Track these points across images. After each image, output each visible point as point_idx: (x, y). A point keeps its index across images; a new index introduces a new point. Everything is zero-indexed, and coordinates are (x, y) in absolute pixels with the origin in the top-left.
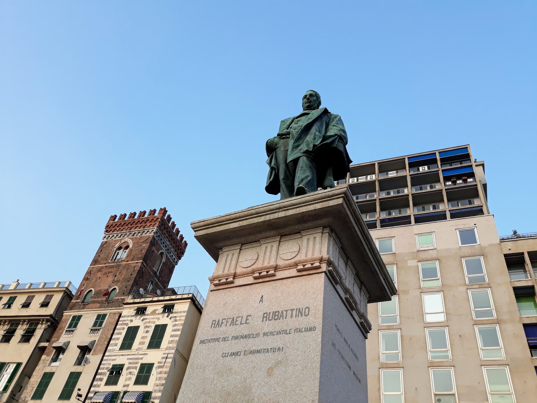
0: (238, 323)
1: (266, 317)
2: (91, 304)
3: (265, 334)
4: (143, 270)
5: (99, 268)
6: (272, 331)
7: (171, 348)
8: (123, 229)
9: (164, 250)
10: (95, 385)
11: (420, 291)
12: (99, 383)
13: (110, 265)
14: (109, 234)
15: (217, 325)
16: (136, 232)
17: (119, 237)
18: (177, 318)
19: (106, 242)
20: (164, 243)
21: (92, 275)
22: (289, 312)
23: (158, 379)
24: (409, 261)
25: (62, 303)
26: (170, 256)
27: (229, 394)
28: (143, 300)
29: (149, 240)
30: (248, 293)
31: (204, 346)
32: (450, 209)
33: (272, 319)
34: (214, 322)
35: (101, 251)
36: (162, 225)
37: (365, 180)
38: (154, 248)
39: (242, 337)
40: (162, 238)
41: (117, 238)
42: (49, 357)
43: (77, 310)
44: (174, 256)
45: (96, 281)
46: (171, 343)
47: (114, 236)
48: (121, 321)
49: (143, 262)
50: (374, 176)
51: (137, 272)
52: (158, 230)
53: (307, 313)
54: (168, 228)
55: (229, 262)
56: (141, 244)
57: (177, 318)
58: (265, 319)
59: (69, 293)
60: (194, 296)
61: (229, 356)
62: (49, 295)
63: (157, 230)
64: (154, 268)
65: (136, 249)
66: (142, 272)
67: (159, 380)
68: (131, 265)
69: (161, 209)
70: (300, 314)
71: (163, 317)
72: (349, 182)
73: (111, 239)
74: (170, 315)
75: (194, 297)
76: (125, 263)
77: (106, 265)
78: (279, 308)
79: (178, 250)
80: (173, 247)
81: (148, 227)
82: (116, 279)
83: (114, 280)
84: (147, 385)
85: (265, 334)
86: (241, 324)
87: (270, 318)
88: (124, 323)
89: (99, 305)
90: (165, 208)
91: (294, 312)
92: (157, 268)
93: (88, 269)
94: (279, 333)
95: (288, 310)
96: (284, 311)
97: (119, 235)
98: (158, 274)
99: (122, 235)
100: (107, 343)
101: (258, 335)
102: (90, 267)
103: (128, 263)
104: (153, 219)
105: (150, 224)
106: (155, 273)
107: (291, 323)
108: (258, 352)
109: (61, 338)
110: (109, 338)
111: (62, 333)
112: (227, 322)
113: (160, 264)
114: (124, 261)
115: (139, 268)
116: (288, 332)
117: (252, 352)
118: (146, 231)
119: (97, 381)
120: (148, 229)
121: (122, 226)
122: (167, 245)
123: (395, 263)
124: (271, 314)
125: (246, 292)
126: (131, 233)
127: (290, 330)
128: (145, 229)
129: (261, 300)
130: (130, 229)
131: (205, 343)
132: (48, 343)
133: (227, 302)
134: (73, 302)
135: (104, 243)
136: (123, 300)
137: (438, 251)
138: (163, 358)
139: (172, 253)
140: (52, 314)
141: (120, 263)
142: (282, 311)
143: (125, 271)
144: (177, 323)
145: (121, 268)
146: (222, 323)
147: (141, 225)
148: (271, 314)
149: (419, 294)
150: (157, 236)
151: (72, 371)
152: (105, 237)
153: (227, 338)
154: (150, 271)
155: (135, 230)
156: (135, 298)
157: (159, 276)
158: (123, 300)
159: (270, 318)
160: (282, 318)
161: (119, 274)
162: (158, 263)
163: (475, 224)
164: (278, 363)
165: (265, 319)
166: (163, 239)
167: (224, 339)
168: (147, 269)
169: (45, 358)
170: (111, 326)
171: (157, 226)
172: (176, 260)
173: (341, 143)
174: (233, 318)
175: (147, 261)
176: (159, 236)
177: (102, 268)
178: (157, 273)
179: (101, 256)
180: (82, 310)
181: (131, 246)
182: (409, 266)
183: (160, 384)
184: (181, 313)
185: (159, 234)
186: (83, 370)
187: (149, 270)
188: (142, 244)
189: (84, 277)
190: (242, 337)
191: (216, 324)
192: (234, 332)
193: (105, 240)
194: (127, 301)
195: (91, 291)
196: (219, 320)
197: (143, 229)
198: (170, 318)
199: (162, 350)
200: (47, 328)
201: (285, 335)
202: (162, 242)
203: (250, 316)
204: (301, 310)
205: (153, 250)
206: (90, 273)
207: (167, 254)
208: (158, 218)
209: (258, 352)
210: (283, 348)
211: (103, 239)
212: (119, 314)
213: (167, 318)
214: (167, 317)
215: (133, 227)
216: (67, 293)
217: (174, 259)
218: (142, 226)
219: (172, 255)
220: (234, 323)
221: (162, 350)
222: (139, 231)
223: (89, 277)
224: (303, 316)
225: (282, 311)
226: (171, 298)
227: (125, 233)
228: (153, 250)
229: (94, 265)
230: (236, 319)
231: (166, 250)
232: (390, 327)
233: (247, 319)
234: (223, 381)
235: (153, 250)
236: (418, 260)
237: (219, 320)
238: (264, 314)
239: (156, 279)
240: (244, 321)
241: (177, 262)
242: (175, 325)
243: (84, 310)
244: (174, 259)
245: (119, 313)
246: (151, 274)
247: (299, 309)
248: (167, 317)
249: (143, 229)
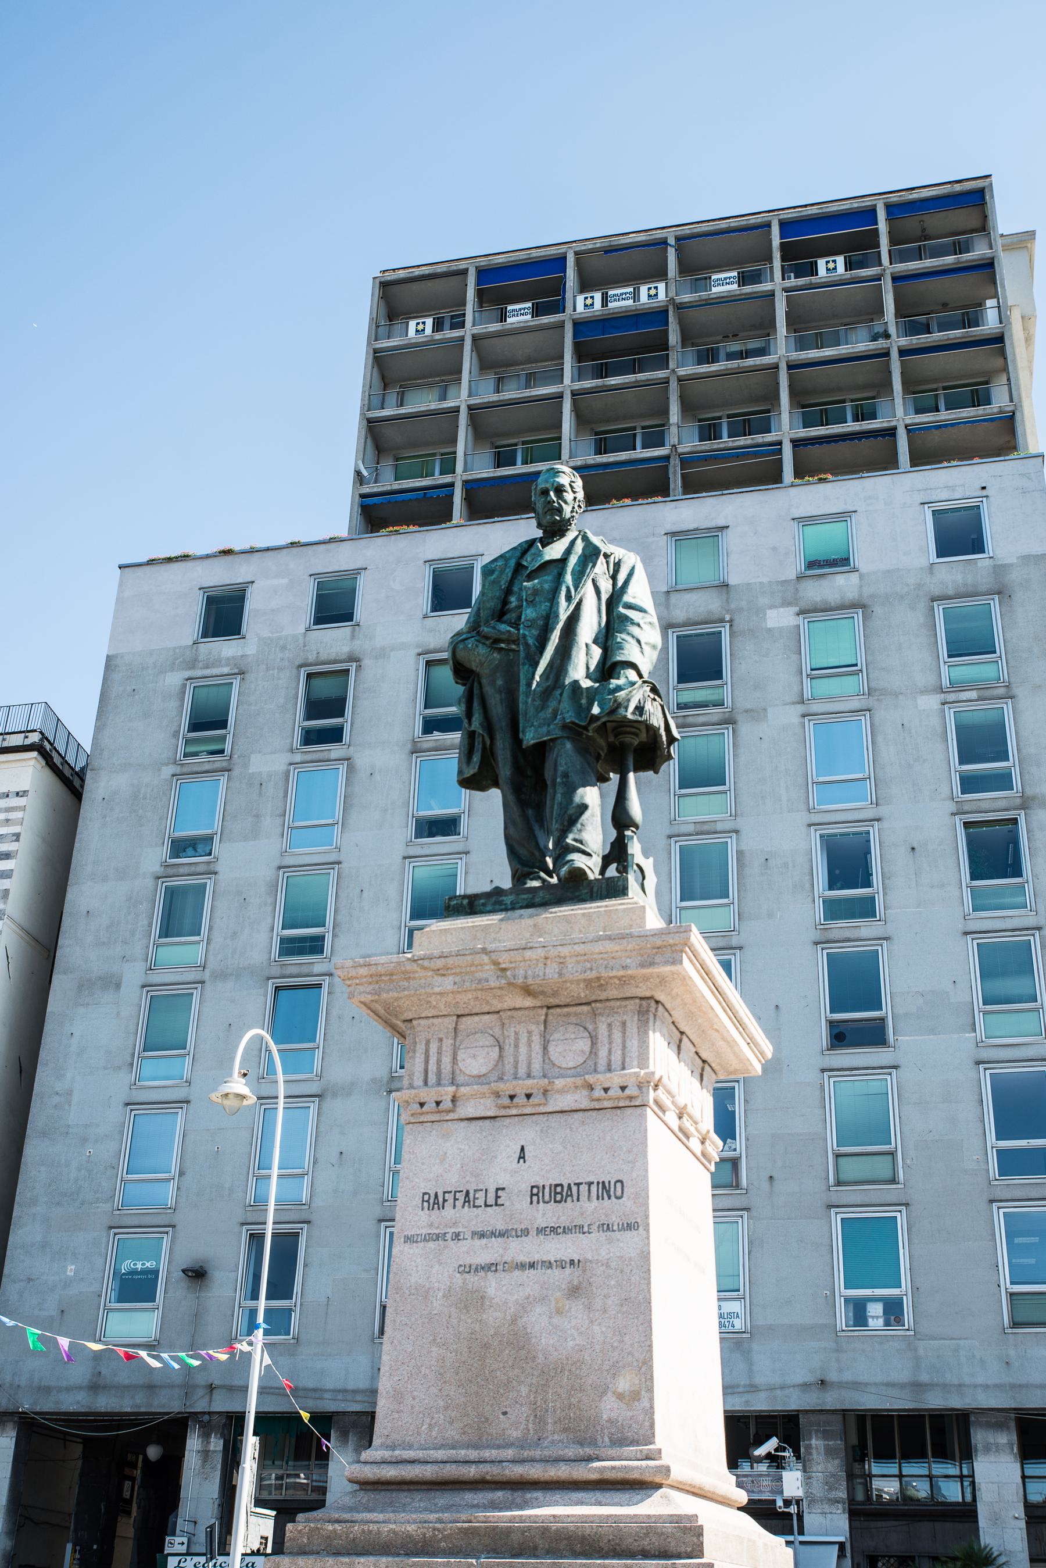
0: (480, 1202)
1: (536, 1193)
3: (540, 1231)
6: (553, 1225)
11: (801, 709)
15: (434, 1204)
22: (584, 1188)
24: (769, 612)
27: (486, 1346)
30: (490, 1138)
31: (416, 1249)
32: (908, 422)
33: (551, 1200)
34: (426, 1197)
37: (630, 302)
39: (493, 1234)
50: (662, 286)
53: (619, 1193)
55: (435, 1058)
58: (535, 1198)
61: (472, 1271)
70: (605, 1193)
72: (575, 310)
75: (46, 743)
78: (562, 1178)
85: (540, 1231)
86: (486, 1205)
87: (547, 1198)
91: (594, 1188)
94: (566, 1230)
95: (581, 1183)
96: (572, 1185)
101: (525, 1232)
107: (590, 1208)
108: (532, 1265)
112: (455, 1199)
116: (586, 1229)
117: (521, 1266)
123: (727, 618)
124: (547, 1190)
125: (484, 1134)
127: (589, 1225)
129: (522, 1157)
131: (417, 1242)
133: (446, 1153)
137: (861, 577)
142: (569, 1185)
146: (445, 1201)
148: (547, 1190)
149: (796, 720)
153: (462, 1234)
159: (547, 1198)
160: (569, 1199)
163: (984, 488)
164: (574, 1291)
165: (535, 1198)
167: (457, 1236)
173: (654, 700)
174: (468, 1192)
182: (770, 630)
184: (7, 800)
190: (493, 1234)
191: (432, 1201)
192: (474, 1222)
196: (436, 1193)
201: (581, 1235)
203: (503, 1189)
204: (607, 1185)
209: (532, 1265)
210: (579, 1261)
220: (472, 1203)
224: (613, 1198)
225: (569, 1185)
230: (474, 1195)
232: (706, 828)
233: (497, 1197)
234: (470, 1321)
236: (798, 608)
237: (436, 1193)
238: (532, 1187)
240: (491, 1200)
247: (603, 1182)
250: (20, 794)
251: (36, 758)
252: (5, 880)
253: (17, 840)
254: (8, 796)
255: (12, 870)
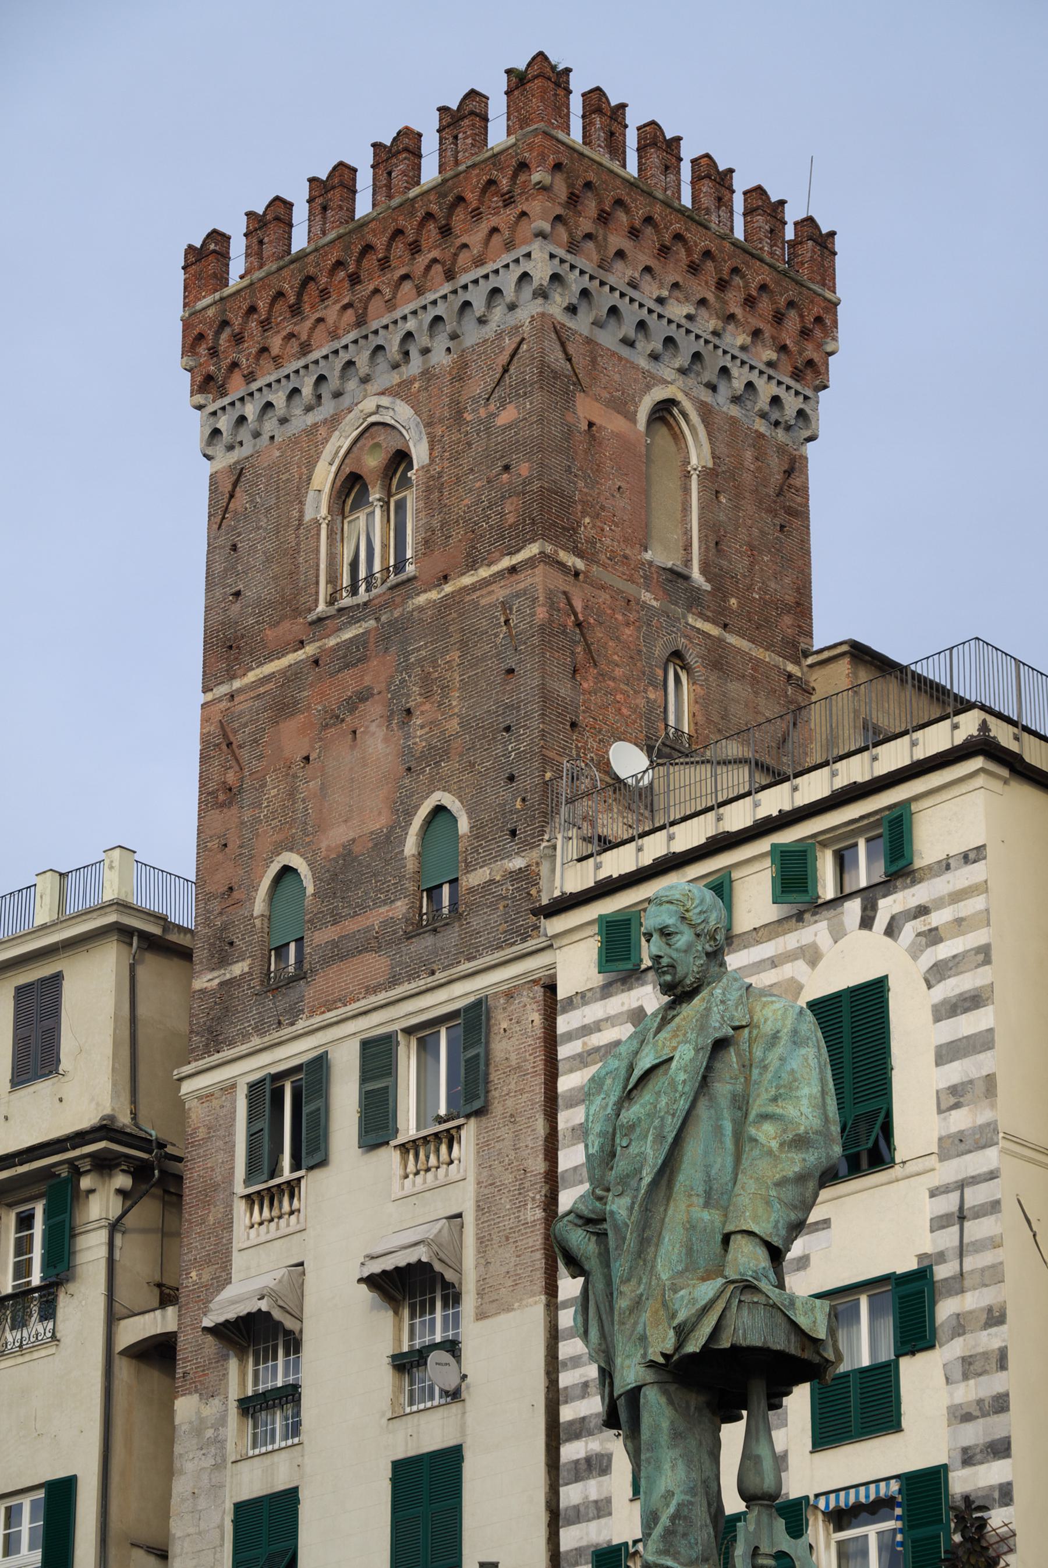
2: (332, 971)
4: (578, 605)
5: (271, 686)
7: (969, 1143)
8: (313, 328)
9: (666, 382)
10: (576, 1508)
12: (591, 1489)
13: (332, 642)
14: (232, 404)
16: (411, 325)
17: (309, 409)
18: (937, 919)
19: (238, 474)
20: (642, 325)
21: (244, 754)
23: (957, 1374)
25: (142, 1011)
26: (736, 400)
28: (655, 848)
29: (524, 370)
35: (234, 548)
36: (573, 200)
38: (586, 409)
40: (615, 299)
41: (301, 421)
42: (216, 1402)
43: (256, 1042)
44: (760, 383)
45: (292, 794)
46: (957, 1106)
47: (269, 405)
48: (570, 1036)
49: (549, 549)
51: (536, 640)
52: (561, 252)
54: (627, 200)
56: (483, 413)
57: (938, 918)
59: (155, 930)
60: (1000, 716)
62: (32, 984)
63: (552, 256)
64: (648, 556)
65: (466, 462)
66: (579, 625)
67: (966, 1377)
68: (475, 604)
69: (517, 80)
71: (838, 935)
73: (265, 437)
74: (882, 903)
76: (434, 595)
77: (310, 650)
79: (778, 318)
80: (731, 317)
81: (479, 262)
82: (419, 735)
83: (407, 752)
84: (902, 1430)
88: (597, 1049)
89: (376, 964)
90: (541, 54)
92: (676, 536)
93: (205, 720)
97: (307, 390)
98: (696, 574)
99: (322, 379)
100: (539, 1214)
102: (210, 696)
103: (448, 588)
104: (491, 182)
105: (484, 227)
106: (678, 577)
109: (238, 1261)
110: (540, 1179)
111: (228, 1225)
113: (686, 490)
114: (417, 584)
115: (541, 613)
118: (477, 297)
119: (577, 1479)
120: (486, 277)
121: (296, 310)
122: (672, 331)
126: (380, 348)
128: (465, 278)
130: (361, 321)
132: (171, 1310)
134: (203, 991)
135: (230, 488)
136: (527, 877)
138: (939, 1223)
139: (735, 372)
140: (108, 1111)
141: (396, 614)
143: (455, 655)
144: (944, 951)
145: (420, 648)
147: (422, 260)
150: (572, 309)
151: (400, 1455)
152: (216, 432)
154: (630, 589)
155: (397, 314)
156: (607, 845)
157: (708, 587)
158: (527, 877)
161: (427, 695)
162: (665, 487)
166: (623, 305)
168: (603, 587)
169: (198, 1412)
170: (522, 1092)
171: (541, 235)
172: (792, 404)
175: (572, 530)
176: (585, 293)
177: (291, 677)
178: (687, 578)
179: (249, 594)
180: (287, 1032)
181: (420, 453)
183: (980, 1402)
184: (948, 876)
185: (575, 282)
186: (463, 1429)
187: (620, 584)
188: (492, 407)
189: (202, 785)
193: (225, 460)
194: (552, 888)
195: (287, 871)
197: (446, 288)
198: (891, 931)
199: (911, 1168)
200: (119, 1212)
202: (628, 329)
205: (591, 424)
206: (229, 745)
207: (706, 396)
208: (523, 166)
211: (209, 457)
212: (539, 991)
213: (865, 933)
214: (867, 922)
215: (377, 291)
216: (143, 935)
217: (776, 400)
218: (435, 261)
219: (750, 385)
221: (911, 1168)
222: (432, 312)
223: (231, 777)
226: (840, 782)
227: (338, 363)
228: (584, 426)
229: (233, 677)
231: (683, 371)
235: (591, 424)
239: (700, 624)
241: (801, 413)
242: (938, 972)
243: (301, 1025)
244: (776, 400)
245: (535, 982)
246: (644, 606)
248: (867, 922)
249: (446, 288)
250: (972, 856)
251: (982, 770)
252: (981, 1057)
253: (987, 961)
254: (948, 867)
255: (991, 1031)
